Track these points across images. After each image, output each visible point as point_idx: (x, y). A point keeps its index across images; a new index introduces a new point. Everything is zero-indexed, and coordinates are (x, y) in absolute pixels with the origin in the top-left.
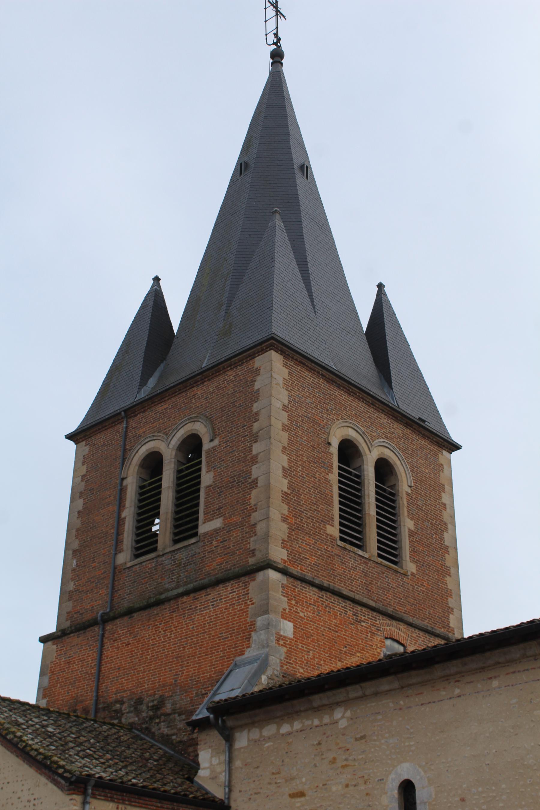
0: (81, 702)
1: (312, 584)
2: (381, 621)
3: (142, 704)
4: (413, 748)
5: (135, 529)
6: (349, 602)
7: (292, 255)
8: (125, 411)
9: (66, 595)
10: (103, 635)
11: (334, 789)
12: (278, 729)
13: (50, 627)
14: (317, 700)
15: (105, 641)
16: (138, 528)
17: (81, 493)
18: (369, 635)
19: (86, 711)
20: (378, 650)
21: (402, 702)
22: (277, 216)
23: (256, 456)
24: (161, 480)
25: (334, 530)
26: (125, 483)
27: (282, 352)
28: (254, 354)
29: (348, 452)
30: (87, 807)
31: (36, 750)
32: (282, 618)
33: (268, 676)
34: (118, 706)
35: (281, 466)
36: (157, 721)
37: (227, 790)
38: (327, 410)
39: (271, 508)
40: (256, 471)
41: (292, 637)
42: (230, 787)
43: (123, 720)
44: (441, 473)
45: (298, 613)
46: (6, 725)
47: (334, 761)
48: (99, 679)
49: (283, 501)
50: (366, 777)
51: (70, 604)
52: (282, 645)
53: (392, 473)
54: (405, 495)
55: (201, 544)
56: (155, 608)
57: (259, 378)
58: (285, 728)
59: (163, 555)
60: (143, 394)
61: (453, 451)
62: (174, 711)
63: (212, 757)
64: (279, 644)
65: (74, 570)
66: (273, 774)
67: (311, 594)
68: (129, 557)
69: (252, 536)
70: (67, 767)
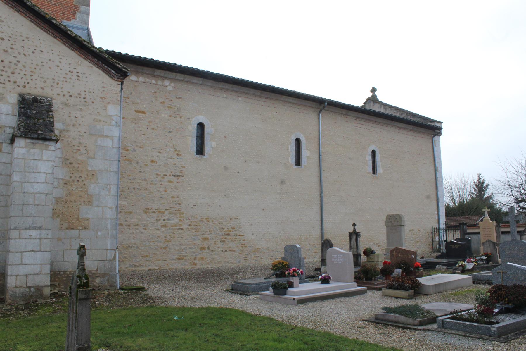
11: (163, 115)
14: (158, 72)
47: (163, 103)
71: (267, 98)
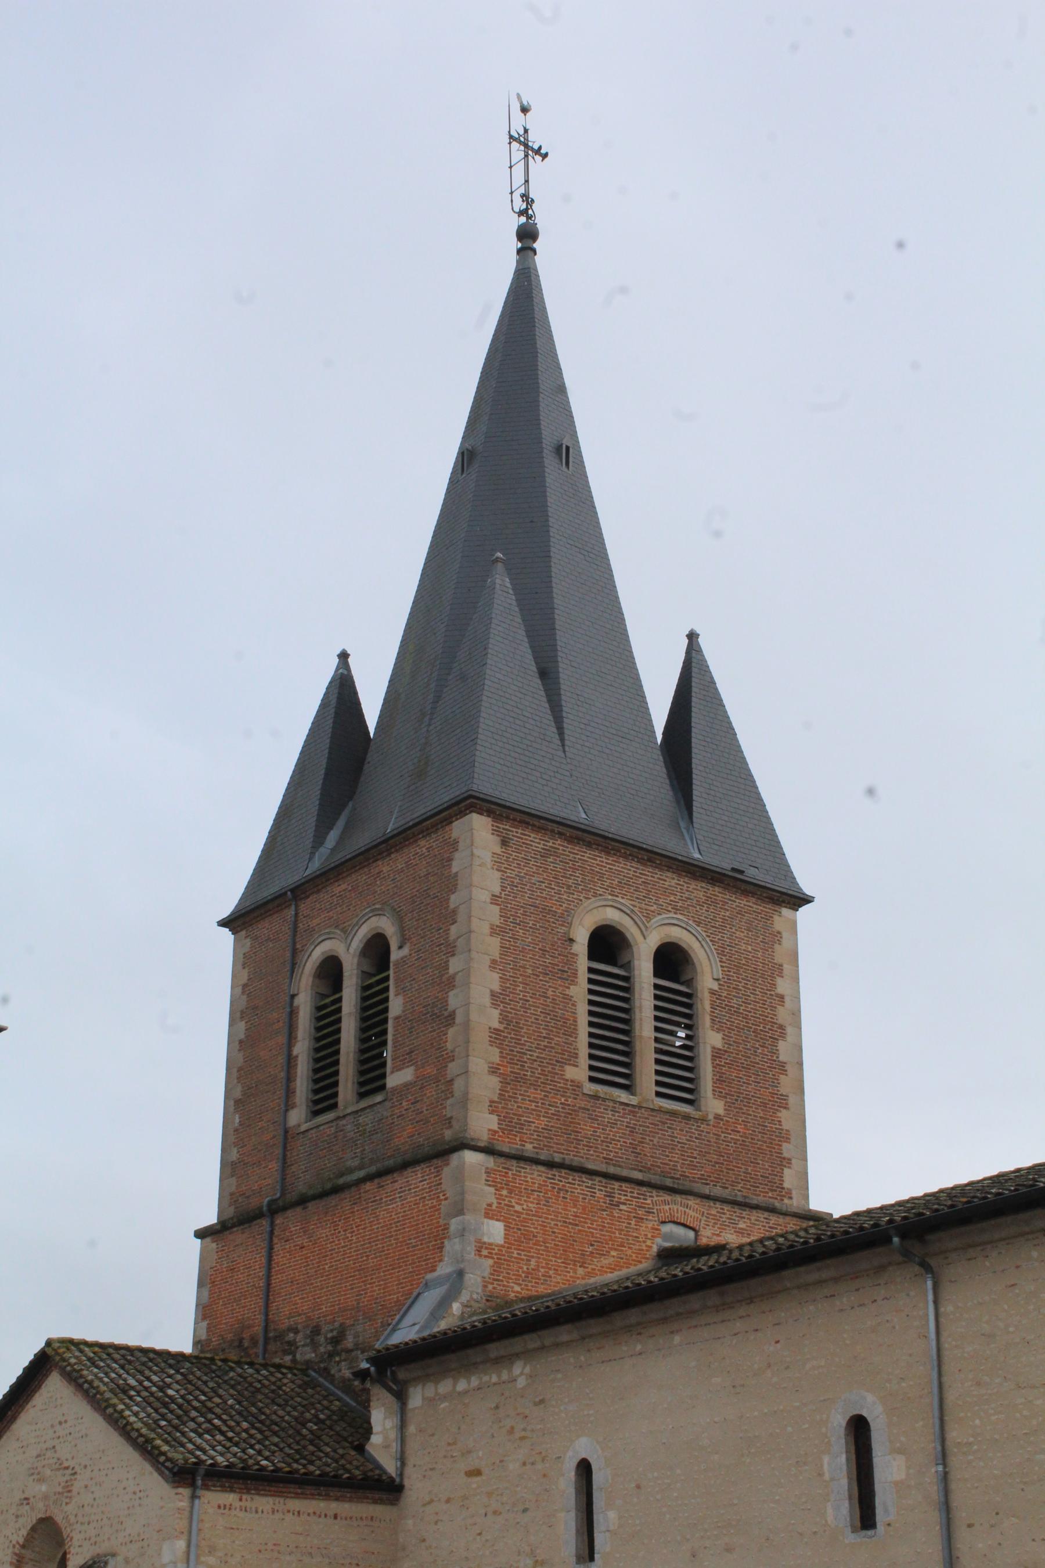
0: (249, 1327)
1: (536, 1162)
2: (655, 1199)
3: (319, 1334)
4: (592, 1419)
5: (311, 1073)
6: (598, 1179)
7: (521, 634)
8: (292, 890)
9: (230, 1169)
10: (272, 1233)
11: (511, 1466)
12: (454, 1386)
14: (495, 1349)
15: (275, 1240)
16: (316, 1071)
17: (242, 1012)
18: (633, 1222)
19: (254, 1341)
20: (649, 1243)
21: (582, 1358)
22: (500, 565)
23: (453, 978)
24: (340, 1000)
25: (579, 1072)
26: (296, 1002)
27: (489, 813)
28: (451, 817)
29: (607, 944)
30: (197, 1502)
31: (138, 1430)
32: (485, 1217)
33: (462, 1304)
34: (292, 1335)
35: (488, 991)
36: (337, 1359)
37: (399, 1463)
38: (569, 887)
39: (470, 1058)
40: (454, 1000)
41: (502, 1242)
42: (402, 1460)
43: (298, 1357)
44: (776, 946)
45: (513, 1207)
46: (108, 1395)
47: (511, 1430)
48: (268, 1296)
49: (492, 1043)
50: (544, 1454)
51: (233, 1181)
52: (486, 1257)
53: (687, 961)
54: (707, 995)
55: (388, 1104)
56: (333, 1196)
57: (457, 855)
58: (462, 1385)
59: (344, 1116)
60: (316, 865)
61: (800, 906)
62: (357, 1347)
63: (385, 1418)
64: (480, 1256)
65: (236, 1130)
66: (449, 1444)
67: (535, 1176)
68: (303, 1116)
69: (448, 1098)
70: (169, 1455)
71: (751, 1301)
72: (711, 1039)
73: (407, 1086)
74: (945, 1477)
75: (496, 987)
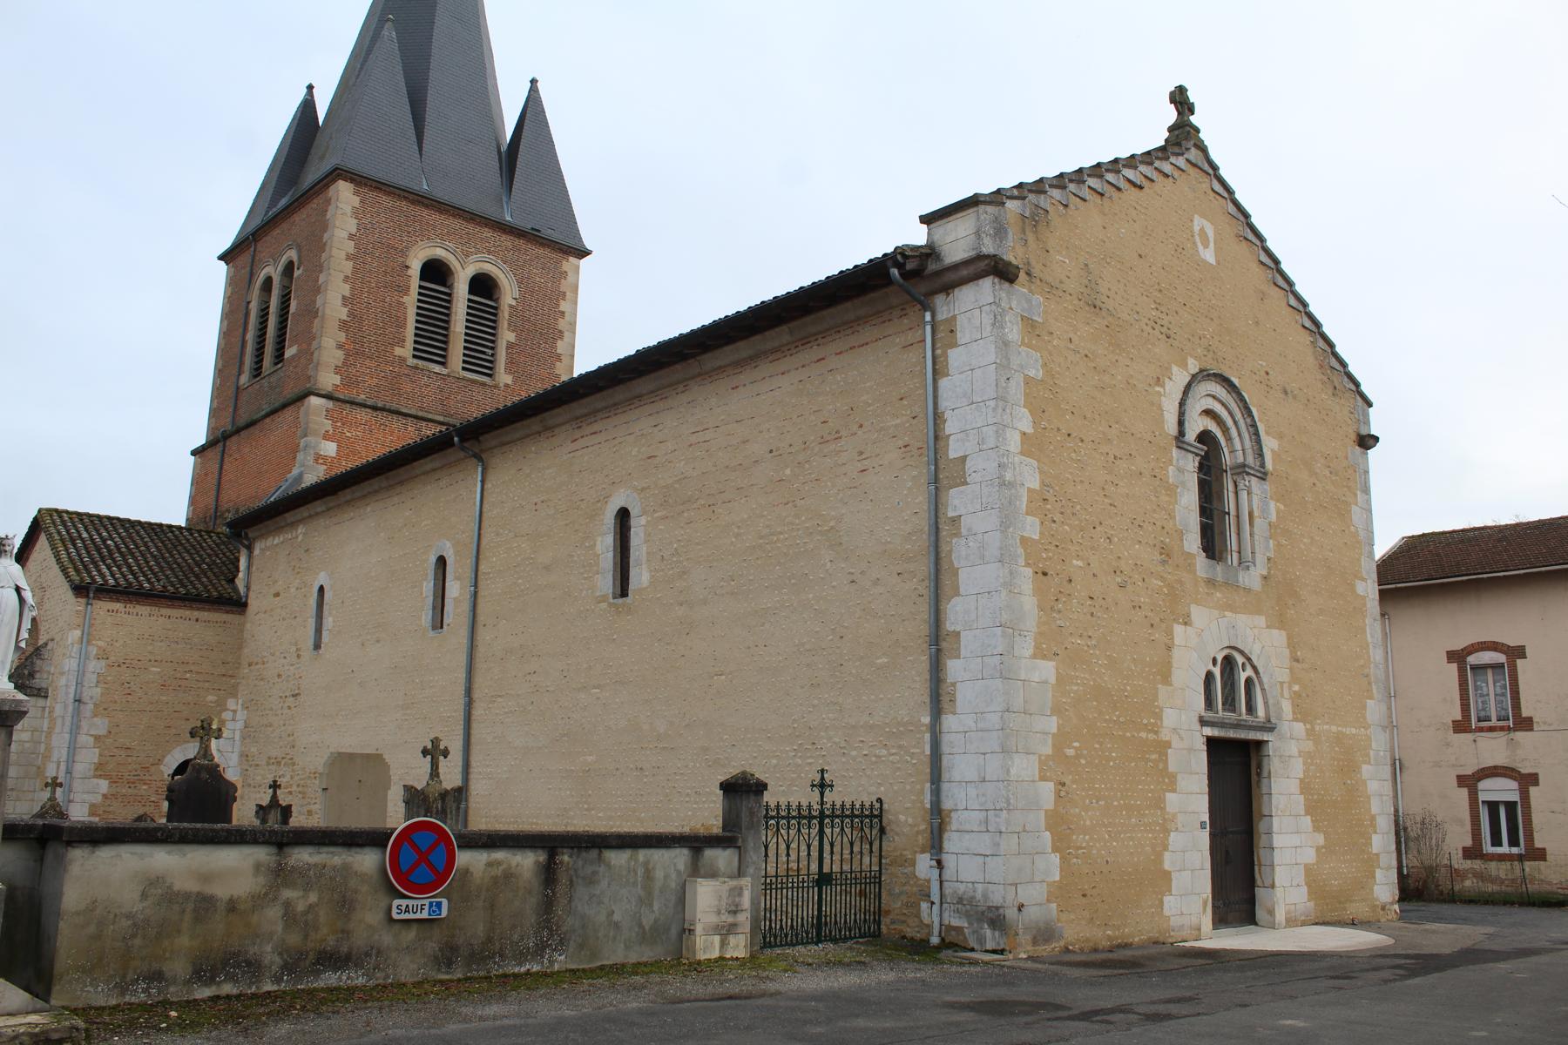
1: (365, 406)
7: (399, 68)
9: (214, 413)
13: (201, 440)
25: (406, 351)
27: (352, 181)
29: (436, 272)
42: (248, 588)
71: (401, 483)
72: (506, 336)
73: (293, 357)
74: (475, 594)
75: (347, 294)
